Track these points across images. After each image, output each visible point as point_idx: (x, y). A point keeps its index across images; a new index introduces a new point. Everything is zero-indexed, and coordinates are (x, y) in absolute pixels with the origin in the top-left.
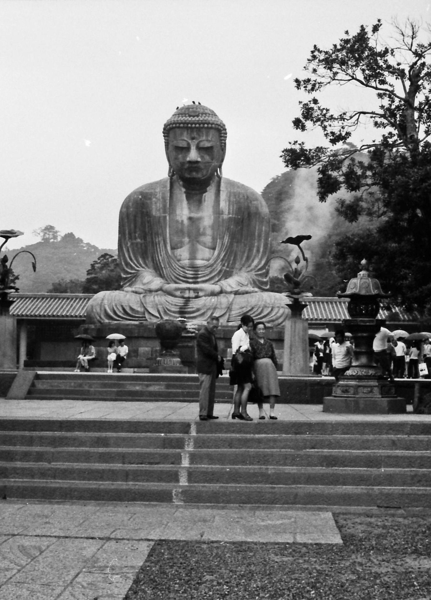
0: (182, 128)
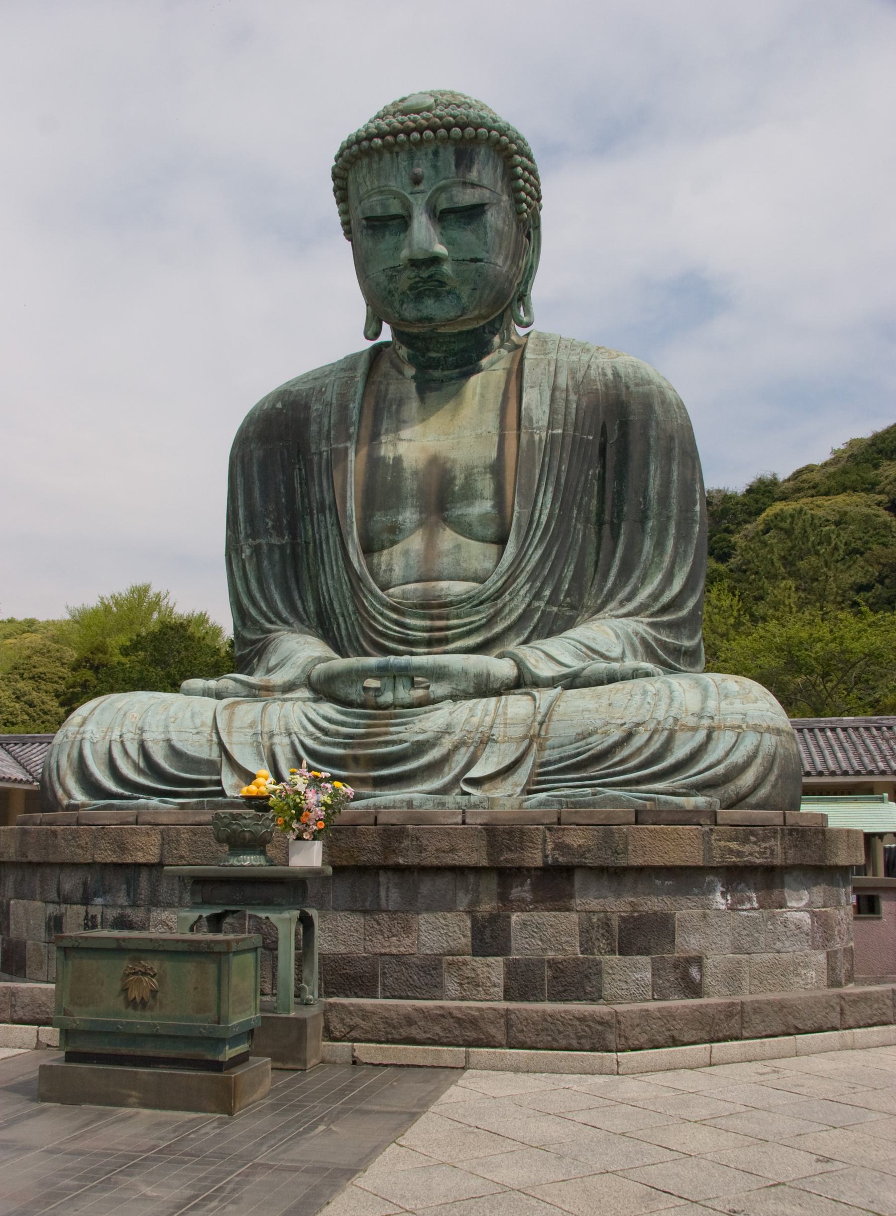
0: (378, 151)
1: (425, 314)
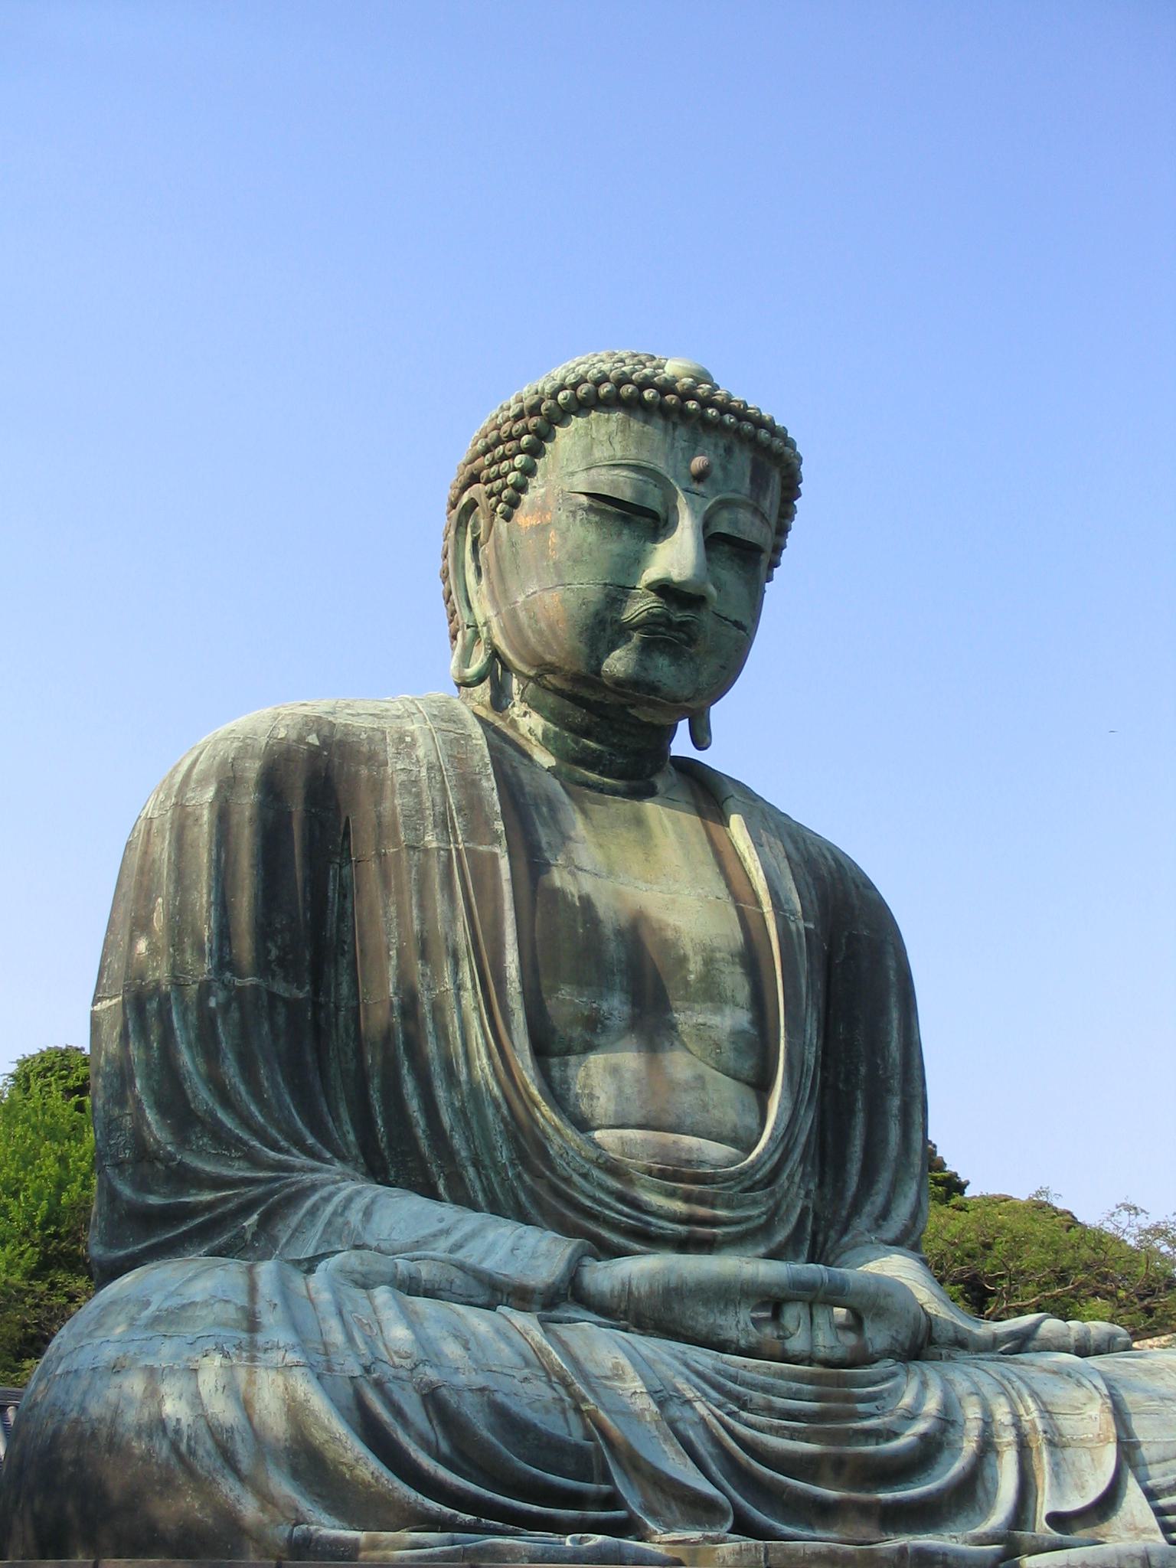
1: (651, 678)
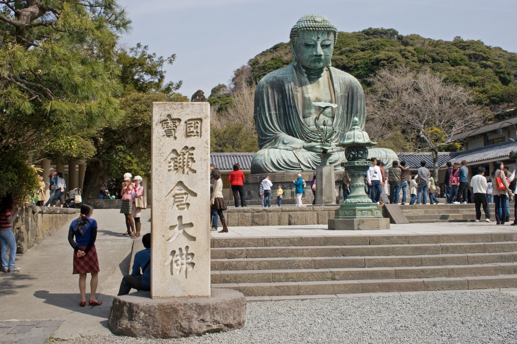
0: (311, 31)
